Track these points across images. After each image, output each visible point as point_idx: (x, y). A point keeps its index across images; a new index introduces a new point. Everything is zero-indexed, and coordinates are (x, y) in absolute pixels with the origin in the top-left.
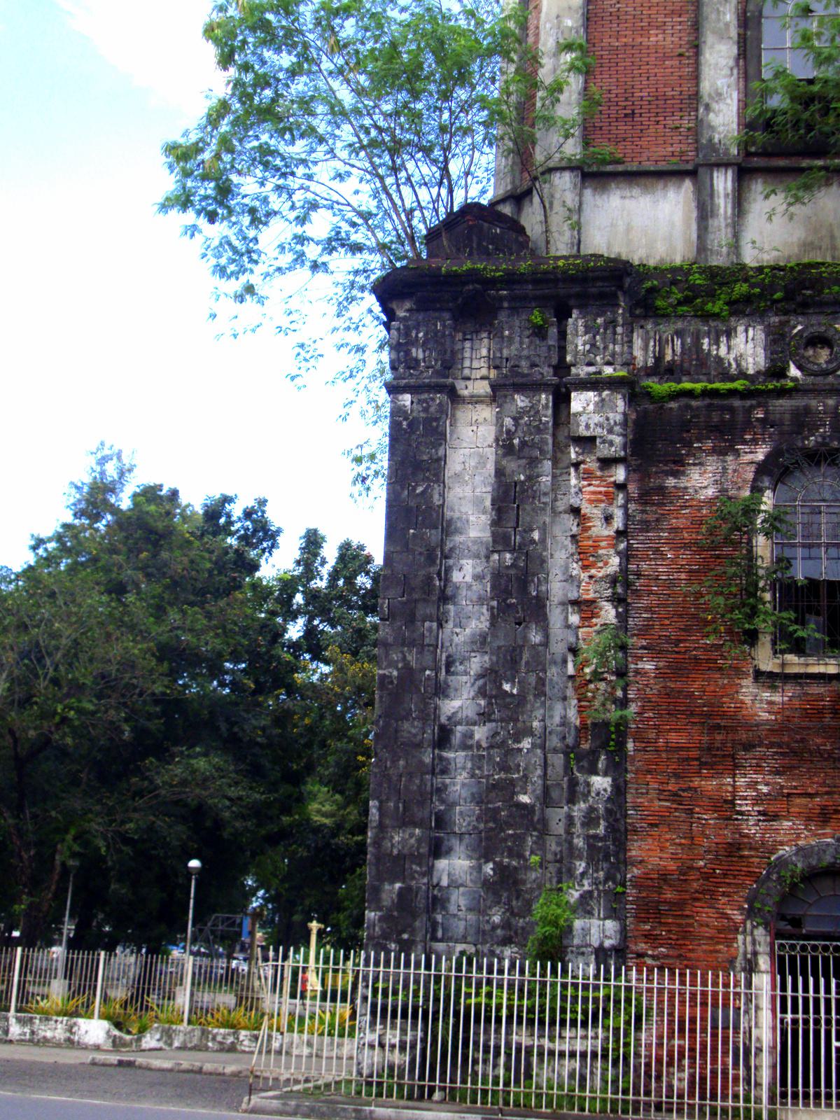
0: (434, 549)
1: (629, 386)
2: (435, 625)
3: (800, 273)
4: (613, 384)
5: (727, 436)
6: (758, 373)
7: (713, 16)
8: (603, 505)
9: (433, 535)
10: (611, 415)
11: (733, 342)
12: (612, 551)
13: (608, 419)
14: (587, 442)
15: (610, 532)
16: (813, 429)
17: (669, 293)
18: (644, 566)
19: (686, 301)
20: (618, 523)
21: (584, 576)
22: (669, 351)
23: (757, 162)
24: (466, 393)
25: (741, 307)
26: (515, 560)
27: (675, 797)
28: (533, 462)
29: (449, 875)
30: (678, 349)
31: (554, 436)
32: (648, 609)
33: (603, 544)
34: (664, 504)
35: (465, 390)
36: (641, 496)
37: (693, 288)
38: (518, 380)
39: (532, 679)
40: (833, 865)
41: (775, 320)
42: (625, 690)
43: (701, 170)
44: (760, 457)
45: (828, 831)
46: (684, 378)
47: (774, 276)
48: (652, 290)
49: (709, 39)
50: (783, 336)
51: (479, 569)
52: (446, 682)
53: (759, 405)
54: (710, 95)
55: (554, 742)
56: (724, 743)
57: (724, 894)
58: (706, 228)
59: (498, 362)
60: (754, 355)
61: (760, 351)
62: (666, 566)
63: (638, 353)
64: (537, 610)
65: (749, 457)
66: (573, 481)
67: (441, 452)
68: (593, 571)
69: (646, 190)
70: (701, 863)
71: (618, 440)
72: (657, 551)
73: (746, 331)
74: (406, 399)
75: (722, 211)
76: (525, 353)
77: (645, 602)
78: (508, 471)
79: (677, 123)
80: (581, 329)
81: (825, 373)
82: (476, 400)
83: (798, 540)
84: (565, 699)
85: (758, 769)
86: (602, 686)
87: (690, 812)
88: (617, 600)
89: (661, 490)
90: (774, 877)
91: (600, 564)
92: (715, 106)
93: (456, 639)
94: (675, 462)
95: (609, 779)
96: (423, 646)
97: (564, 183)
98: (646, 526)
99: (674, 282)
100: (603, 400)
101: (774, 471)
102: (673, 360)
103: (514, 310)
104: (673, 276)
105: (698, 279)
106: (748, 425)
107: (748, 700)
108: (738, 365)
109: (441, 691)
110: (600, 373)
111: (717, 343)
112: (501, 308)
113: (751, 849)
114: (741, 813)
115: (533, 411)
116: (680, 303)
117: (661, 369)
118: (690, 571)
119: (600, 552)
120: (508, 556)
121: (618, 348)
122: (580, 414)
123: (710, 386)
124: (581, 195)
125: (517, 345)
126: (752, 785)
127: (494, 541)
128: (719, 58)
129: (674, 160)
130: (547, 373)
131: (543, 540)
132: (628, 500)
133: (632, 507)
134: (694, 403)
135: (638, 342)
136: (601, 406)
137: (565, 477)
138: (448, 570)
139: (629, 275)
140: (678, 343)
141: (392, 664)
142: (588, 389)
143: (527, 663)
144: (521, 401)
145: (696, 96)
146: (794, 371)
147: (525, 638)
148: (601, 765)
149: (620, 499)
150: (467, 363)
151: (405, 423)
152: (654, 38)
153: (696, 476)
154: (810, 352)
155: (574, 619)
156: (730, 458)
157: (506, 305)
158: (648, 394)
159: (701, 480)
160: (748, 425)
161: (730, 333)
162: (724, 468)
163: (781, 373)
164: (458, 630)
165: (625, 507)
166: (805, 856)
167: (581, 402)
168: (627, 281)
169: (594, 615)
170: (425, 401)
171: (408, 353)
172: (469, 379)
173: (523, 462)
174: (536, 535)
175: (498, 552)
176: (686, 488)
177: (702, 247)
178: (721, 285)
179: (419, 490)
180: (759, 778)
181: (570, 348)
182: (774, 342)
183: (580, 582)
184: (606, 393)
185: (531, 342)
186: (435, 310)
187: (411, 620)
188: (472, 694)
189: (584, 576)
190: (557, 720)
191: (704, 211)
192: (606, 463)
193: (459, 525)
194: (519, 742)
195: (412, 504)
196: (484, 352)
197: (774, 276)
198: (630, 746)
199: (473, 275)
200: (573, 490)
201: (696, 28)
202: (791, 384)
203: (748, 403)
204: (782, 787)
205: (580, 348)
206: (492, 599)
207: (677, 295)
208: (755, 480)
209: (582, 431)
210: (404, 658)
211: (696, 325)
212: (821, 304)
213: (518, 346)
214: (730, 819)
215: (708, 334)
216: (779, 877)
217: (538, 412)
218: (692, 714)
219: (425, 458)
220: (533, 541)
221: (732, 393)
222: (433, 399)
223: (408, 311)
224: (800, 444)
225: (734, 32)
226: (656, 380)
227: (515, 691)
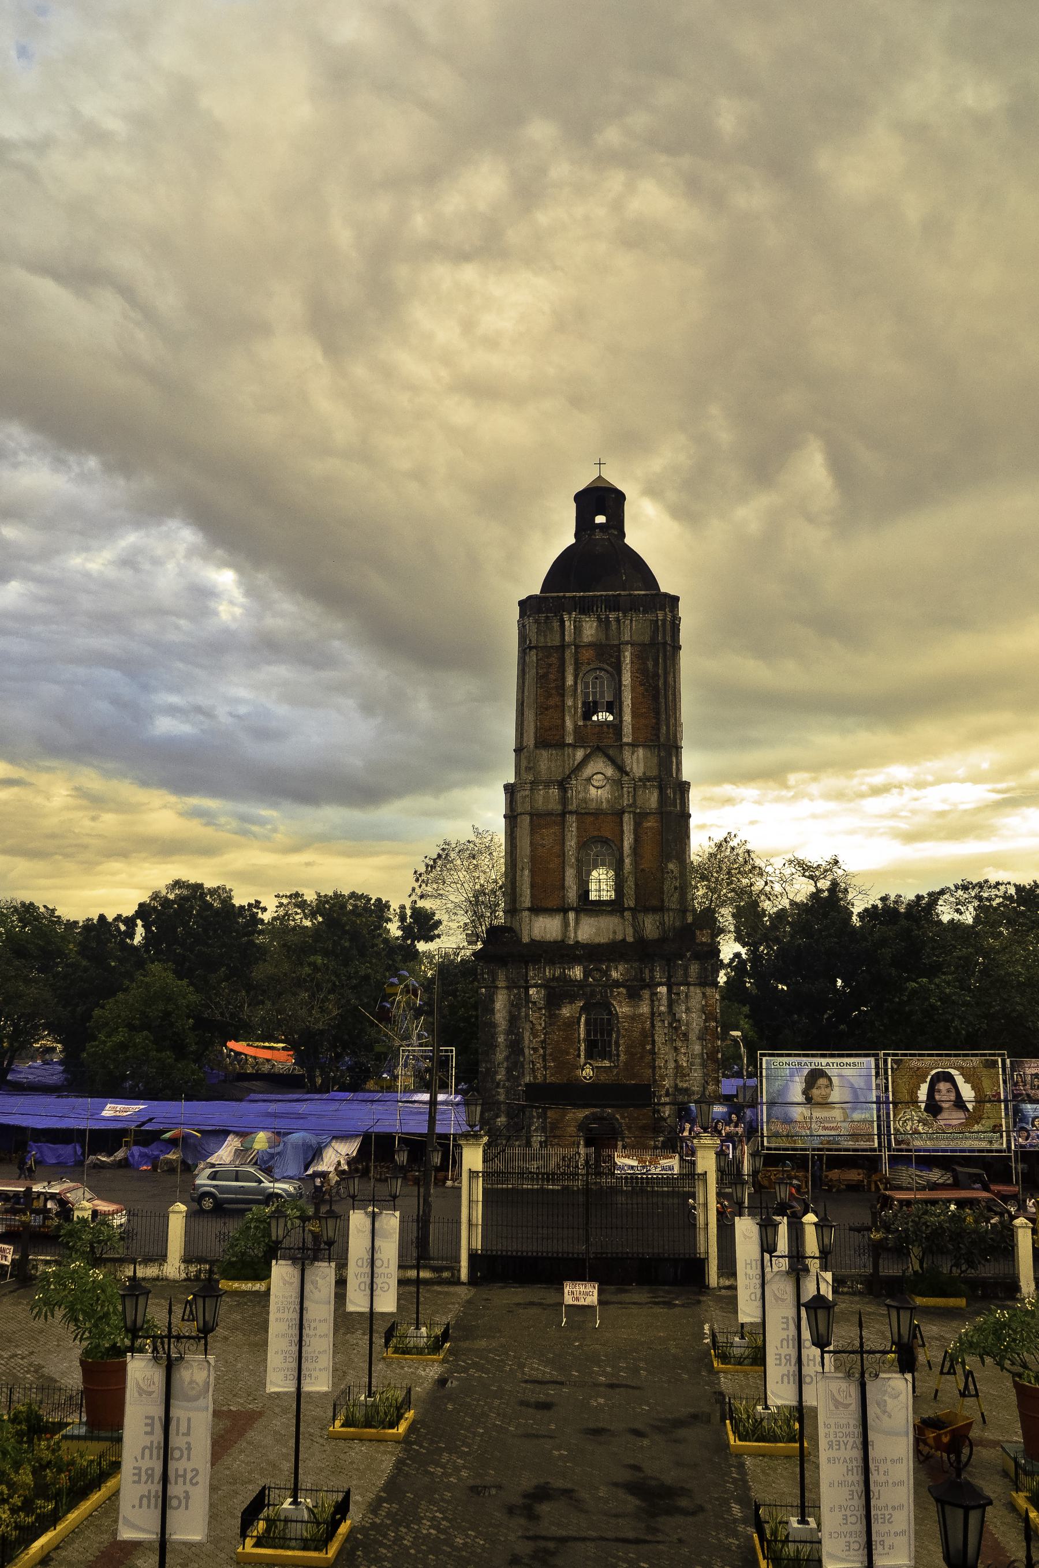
5: (572, 999)
14: (534, 1003)
28: (520, 1009)
49: (567, 868)
88: (543, 1048)
89: (555, 1014)
98: (551, 1025)
109: (496, 1073)
115: (519, 994)
136: (537, 992)
159: (566, 1012)
191: (566, 924)
201: (564, 862)
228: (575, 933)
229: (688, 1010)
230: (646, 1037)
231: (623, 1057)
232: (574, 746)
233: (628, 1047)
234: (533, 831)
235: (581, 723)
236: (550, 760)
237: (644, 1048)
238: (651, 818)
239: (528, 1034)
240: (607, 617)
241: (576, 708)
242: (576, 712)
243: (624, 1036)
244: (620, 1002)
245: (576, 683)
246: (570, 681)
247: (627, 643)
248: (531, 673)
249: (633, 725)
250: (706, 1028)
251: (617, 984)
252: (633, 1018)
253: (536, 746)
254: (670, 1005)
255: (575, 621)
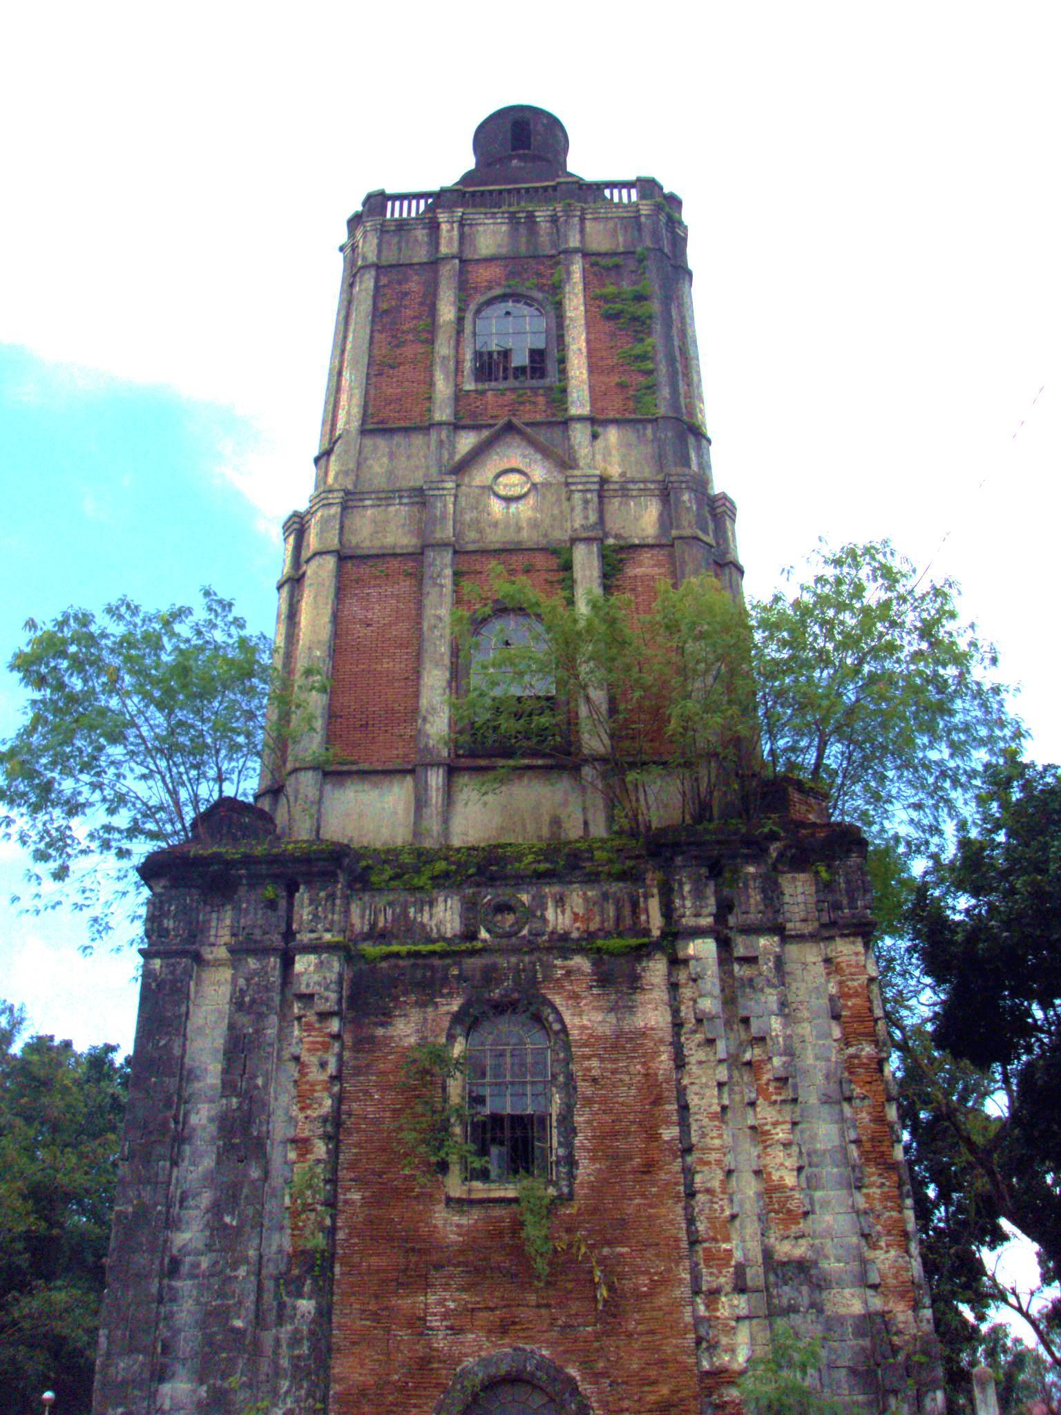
0: (172, 1095)
1: (346, 951)
2: (168, 1163)
3: (490, 852)
4: (331, 948)
6: (455, 936)
7: (432, 649)
8: (319, 1053)
9: (171, 1083)
10: (328, 975)
11: (434, 911)
12: (326, 1094)
13: (325, 978)
14: (308, 998)
15: (324, 1077)
16: (498, 983)
17: (382, 871)
18: (355, 1106)
19: (397, 877)
20: (332, 1068)
21: (301, 1116)
22: (382, 919)
23: (464, 762)
24: (210, 957)
25: (442, 881)
26: (240, 1104)
27: (375, 1317)
28: (261, 1016)
29: (172, 1398)
30: (389, 917)
31: (282, 992)
32: (358, 1145)
33: (318, 1088)
34: (374, 1052)
35: (208, 954)
36: (355, 1045)
37: (400, 866)
38: (252, 946)
39: (250, 1211)
40: (508, 1373)
41: (469, 891)
42: (334, 1218)
43: (418, 769)
44: (455, 1008)
45: (507, 1341)
46: (394, 942)
47: (469, 855)
48: (368, 868)
49: (428, 665)
50: (475, 904)
51: (213, 1113)
52: (178, 1214)
53: (455, 964)
54: (427, 710)
55: (269, 1269)
56: (416, 1263)
57: (415, 1406)
58: (421, 816)
59: (235, 931)
60: (452, 920)
61: (457, 917)
62: (369, 1106)
63: (356, 919)
64: (258, 1148)
65: (446, 1008)
66: (296, 1033)
67: (184, 1009)
68: (309, 1112)
69: (375, 785)
70: (396, 1377)
71: (333, 996)
72: (366, 1092)
73: (446, 901)
74: (157, 963)
75: (434, 801)
76: (260, 922)
77: (355, 1138)
78: (239, 1024)
79: (402, 732)
80: (306, 902)
81: (509, 935)
82: (218, 963)
83: (508, 1078)
84: (282, 1228)
85: (446, 1287)
86: (312, 1215)
87: (388, 1330)
88: (328, 1138)
89: (372, 1039)
90: (459, 1387)
91: (316, 1106)
92: (430, 718)
93: (190, 1176)
94: (384, 1014)
95: (313, 1302)
96: (157, 1183)
97: (307, 782)
98: (358, 1071)
99: (385, 862)
100: (322, 962)
101: (467, 1021)
102: (385, 927)
103: (252, 886)
104: (389, 856)
105: (406, 859)
106: (445, 980)
107: (440, 1223)
108: (438, 930)
109: (172, 1224)
110: (320, 938)
111: (422, 911)
112: (240, 884)
113: (440, 1362)
114: (432, 1329)
115: (263, 971)
116: (391, 879)
117: (377, 935)
118: (394, 1110)
119: (316, 1095)
120: (234, 1100)
121: (336, 917)
122: (301, 974)
123: (414, 948)
124: (321, 791)
125: (251, 916)
126: (441, 1303)
127: (223, 1087)
128: (434, 680)
129: (399, 761)
130: (276, 939)
131: (266, 1085)
132: (343, 1047)
133: (347, 1054)
134: (401, 963)
135: (355, 909)
137: (290, 1029)
138: (186, 1115)
139: (347, 855)
140: (389, 911)
141: (130, 1202)
142: (310, 953)
143: (247, 1197)
144: (253, 963)
145: (416, 710)
146: (484, 934)
147: (246, 1175)
148: (307, 1288)
149: (336, 1047)
150: (213, 932)
151: (154, 985)
152: (387, 664)
153: (402, 1026)
154: (499, 917)
155: (292, 1155)
156: (430, 1009)
157: (244, 882)
158: (363, 956)
159: (405, 1030)
160: (445, 980)
161: (431, 904)
162: (425, 1019)
163: (471, 936)
164: (192, 1168)
165: (340, 1056)
166: (485, 1366)
167: (303, 963)
168: (346, 861)
169: (308, 1152)
170: (173, 965)
171: (160, 924)
172: (214, 945)
173: (253, 1016)
174: (260, 1081)
175: (226, 1096)
176: (392, 1037)
177: (416, 834)
178: (425, 863)
179: (162, 1043)
180: (447, 1295)
181: (296, 917)
182: (467, 909)
183: (297, 1123)
184: (324, 956)
185: (264, 914)
186: (186, 886)
187: (147, 1162)
188: (201, 1227)
189: (301, 1116)
190: (274, 1248)
191: (420, 803)
192: (324, 1016)
193: (198, 1072)
194: (236, 1270)
195: (156, 1055)
196: (228, 922)
197: (469, 855)
198: (337, 1269)
199: (216, 857)
200: (294, 1041)
201: (419, 658)
202: (479, 945)
203: (448, 961)
204: (467, 1302)
205: (305, 917)
206: (219, 1139)
207: (389, 872)
208: (450, 1029)
209: (303, 989)
210: (139, 1196)
211: (403, 896)
212: (505, 877)
213: (255, 917)
214: (422, 1334)
215: (414, 904)
216: (463, 1387)
217: (266, 973)
218: (392, 1239)
219: (169, 1014)
220: (257, 1087)
221: (433, 953)
222: (179, 963)
223: (164, 887)
224: (487, 996)
225: (447, 661)
226: (370, 943)
227: (234, 1223)
228: (446, 820)
229: (785, 1009)
230: (658, 1101)
231: (586, 1170)
232: (457, 426)
233: (606, 1137)
234: (340, 592)
235: (469, 386)
236: (392, 456)
237: (654, 1137)
238: (646, 556)
239: (284, 1099)
240: (531, 216)
241: (458, 363)
242: (458, 370)
243: (589, 1101)
244: (575, 997)
245: (460, 320)
246: (447, 313)
247: (576, 251)
248: (364, 306)
249: (592, 389)
250: (850, 1065)
251: (563, 945)
252: (622, 1044)
253: (364, 432)
254: (729, 1000)
255: (462, 225)
